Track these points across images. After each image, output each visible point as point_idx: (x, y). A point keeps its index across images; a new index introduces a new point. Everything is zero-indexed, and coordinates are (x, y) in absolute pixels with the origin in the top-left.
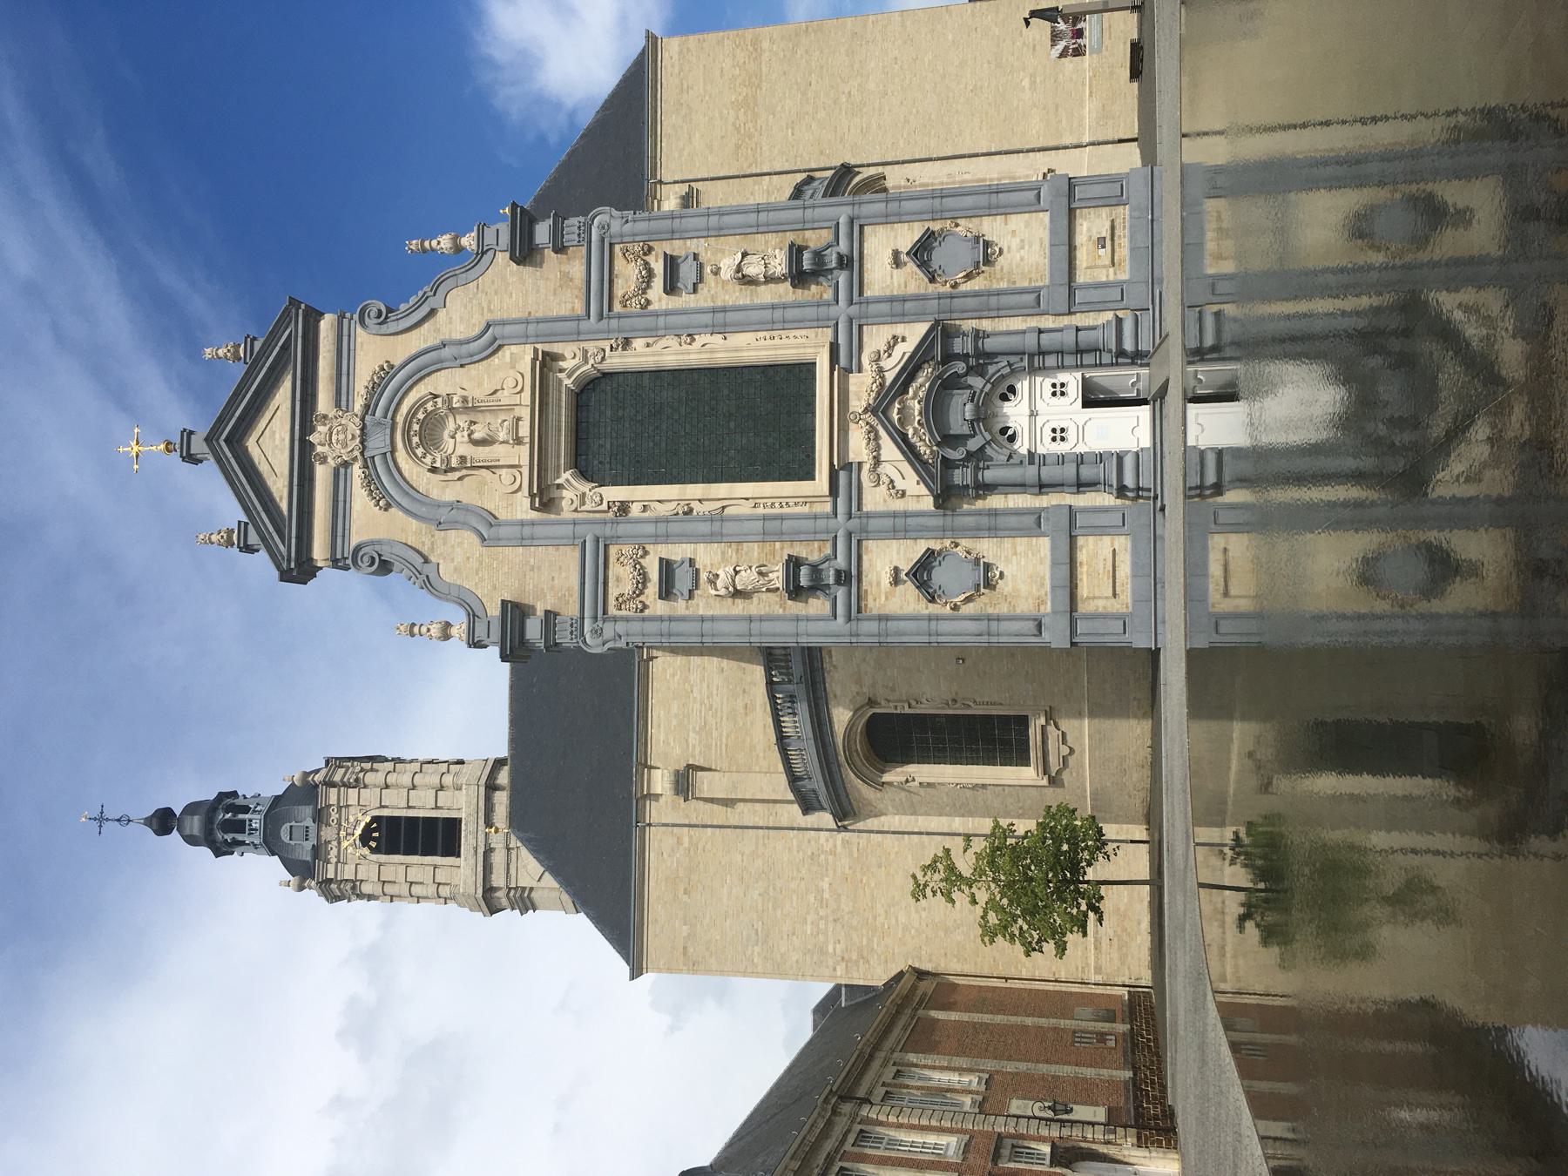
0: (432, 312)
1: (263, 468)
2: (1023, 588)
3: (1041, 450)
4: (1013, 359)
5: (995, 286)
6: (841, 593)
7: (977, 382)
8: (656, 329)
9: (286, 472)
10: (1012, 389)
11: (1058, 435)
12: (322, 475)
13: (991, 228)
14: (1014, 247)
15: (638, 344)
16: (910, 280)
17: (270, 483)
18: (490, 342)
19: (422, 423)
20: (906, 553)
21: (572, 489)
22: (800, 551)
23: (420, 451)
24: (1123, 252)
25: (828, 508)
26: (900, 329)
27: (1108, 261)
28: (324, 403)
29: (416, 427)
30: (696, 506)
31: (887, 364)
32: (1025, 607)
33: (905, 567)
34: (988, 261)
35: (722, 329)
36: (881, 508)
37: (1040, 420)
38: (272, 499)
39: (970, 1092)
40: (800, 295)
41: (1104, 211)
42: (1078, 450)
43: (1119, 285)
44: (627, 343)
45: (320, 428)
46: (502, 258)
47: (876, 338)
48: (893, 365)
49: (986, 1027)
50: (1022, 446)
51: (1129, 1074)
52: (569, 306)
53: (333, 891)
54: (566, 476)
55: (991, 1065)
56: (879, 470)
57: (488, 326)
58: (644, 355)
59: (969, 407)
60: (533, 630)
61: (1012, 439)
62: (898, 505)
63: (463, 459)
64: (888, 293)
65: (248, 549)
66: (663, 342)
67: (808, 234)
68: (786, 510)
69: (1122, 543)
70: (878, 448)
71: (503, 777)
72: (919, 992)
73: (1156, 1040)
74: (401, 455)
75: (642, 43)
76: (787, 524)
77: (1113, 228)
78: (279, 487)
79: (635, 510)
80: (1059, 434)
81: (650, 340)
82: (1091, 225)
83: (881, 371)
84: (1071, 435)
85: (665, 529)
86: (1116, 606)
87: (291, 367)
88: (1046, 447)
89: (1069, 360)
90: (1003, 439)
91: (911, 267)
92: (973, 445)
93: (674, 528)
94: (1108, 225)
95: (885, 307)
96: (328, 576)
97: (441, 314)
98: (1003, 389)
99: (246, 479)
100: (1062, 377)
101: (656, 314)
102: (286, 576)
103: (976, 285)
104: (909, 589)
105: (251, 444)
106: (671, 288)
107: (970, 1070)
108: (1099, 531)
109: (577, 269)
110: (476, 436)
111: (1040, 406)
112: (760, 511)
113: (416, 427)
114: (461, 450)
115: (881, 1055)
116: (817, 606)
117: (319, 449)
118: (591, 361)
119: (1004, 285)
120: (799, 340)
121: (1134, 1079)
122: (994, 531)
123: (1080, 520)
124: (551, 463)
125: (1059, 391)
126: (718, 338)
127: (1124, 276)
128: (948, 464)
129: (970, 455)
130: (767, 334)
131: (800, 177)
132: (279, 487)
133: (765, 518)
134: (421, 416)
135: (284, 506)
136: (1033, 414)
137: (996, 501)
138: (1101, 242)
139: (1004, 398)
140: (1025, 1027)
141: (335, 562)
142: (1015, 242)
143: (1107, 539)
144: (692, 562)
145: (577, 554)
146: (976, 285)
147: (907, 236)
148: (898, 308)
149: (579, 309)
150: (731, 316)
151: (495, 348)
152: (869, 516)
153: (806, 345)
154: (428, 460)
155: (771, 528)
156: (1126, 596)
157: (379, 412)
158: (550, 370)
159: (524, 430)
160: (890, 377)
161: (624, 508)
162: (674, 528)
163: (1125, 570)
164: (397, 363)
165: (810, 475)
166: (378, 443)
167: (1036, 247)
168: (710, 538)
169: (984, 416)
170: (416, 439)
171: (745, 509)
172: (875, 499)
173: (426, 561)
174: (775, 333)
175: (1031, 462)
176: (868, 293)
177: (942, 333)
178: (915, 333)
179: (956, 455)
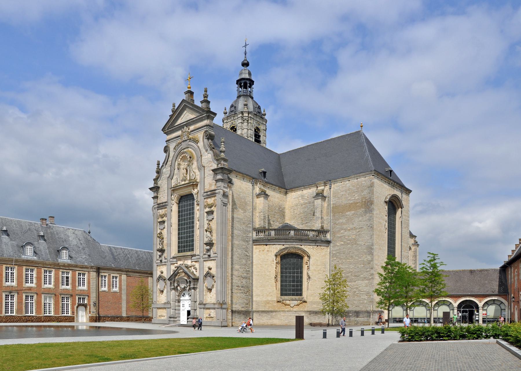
13: (214, 290)
15: (198, 207)
22: (166, 252)
31: (192, 268)
44: (198, 205)
47: (197, 265)
55: (124, 292)
57: (204, 167)
58: (196, 208)
83: (191, 267)
84: (183, 308)
124: (178, 191)
136: (186, 300)
138: (210, 315)
142: (211, 296)
144: (164, 228)
146: (205, 288)
155: (169, 245)
163: (163, 318)
165: (179, 252)
173: (166, 164)
177: (196, 280)
178: (197, 274)
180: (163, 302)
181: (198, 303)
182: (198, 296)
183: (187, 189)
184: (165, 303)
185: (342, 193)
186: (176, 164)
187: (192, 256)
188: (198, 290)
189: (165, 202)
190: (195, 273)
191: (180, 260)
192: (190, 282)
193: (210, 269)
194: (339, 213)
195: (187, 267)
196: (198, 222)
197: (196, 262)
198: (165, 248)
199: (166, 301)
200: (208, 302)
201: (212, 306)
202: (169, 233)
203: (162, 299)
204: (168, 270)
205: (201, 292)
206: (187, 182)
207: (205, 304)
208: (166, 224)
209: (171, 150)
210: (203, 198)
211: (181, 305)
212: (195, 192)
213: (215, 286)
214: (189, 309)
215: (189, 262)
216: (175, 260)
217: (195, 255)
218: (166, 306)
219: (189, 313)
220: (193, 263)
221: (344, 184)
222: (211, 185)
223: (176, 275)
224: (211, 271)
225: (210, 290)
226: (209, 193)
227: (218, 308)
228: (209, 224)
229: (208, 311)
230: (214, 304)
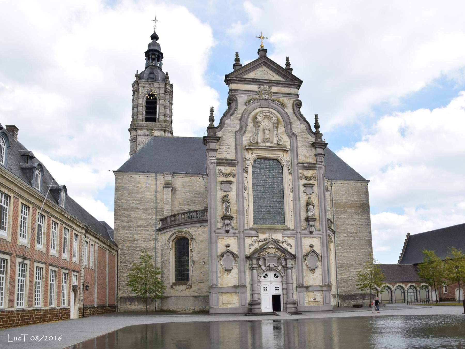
0: (299, 120)
1: (256, 71)
2: (225, 280)
3: (261, 284)
4: (285, 277)
5: (304, 272)
6: (223, 231)
7: (280, 268)
8: (294, 182)
9: (256, 78)
10: (277, 277)
11: (265, 289)
12: (254, 87)
13: (319, 271)
14: (314, 277)
15: (290, 177)
16: (306, 249)
17: (252, 73)
18: (291, 135)
19: (269, 116)
20: (234, 248)
21: (251, 157)
23: (261, 115)
24: (312, 304)
25: (246, 227)
26: (293, 247)
27: (309, 300)
28: (275, 89)
29: (268, 114)
30: (246, 192)
32: (220, 281)
33: (230, 248)
34: (311, 270)
35: (294, 199)
36: (246, 242)
37: (269, 284)
38: (248, 73)
39: (89, 265)
40: (303, 221)
41: (322, 299)
42: (261, 294)
43: (304, 303)
45: (268, 87)
46: (313, 140)
47: (292, 241)
48: (284, 245)
49: (105, 269)
50: (262, 279)
51: (96, 306)
52: (300, 158)
53: (136, 85)
54: (255, 156)
55: (96, 270)
56: (257, 242)
59: (273, 266)
60: (212, 145)
61: (264, 277)
62: (247, 246)
63: (259, 127)
64: (303, 244)
65: (234, 66)
66: (291, 184)
67: (319, 223)
68: (245, 216)
69: (237, 305)
70: (262, 241)
71: (168, 135)
72: (113, 251)
73: (104, 313)
74: (259, 109)
75: (367, 179)
76: (242, 216)
77: (318, 301)
78: (251, 75)
79: (245, 175)
80: (265, 289)
81: (291, 180)
82: (319, 296)
84: (265, 292)
85: (241, 182)
86: (220, 303)
87: (284, 80)
88: (262, 286)
89: (285, 291)
90: (264, 274)
91: (309, 249)
92: (263, 267)
93: (240, 185)
94: (319, 300)
95: (299, 243)
96: (227, 88)
97: (299, 122)
98: (278, 274)
99: (253, 66)
100: (280, 289)
101: (298, 182)
102: (227, 76)
103: (305, 268)
104: (225, 249)
105: (264, 68)
106: (305, 185)
107: (95, 265)
108: (240, 300)
109: (311, 160)
110: (266, 131)
111: (273, 284)
112: (245, 210)
113: (268, 114)
114: (261, 126)
115: (96, 240)
116: (220, 225)
117: (262, 87)
118: (286, 163)
119: (304, 274)
120: (291, 221)
121: (94, 307)
122: (240, 271)
123: (243, 295)
124: (258, 152)
125: (277, 289)
126: (291, 199)
127: (306, 304)
128: (258, 260)
129: (260, 266)
130: (293, 212)
131: (332, 221)
132: (251, 75)
133: (243, 211)
134: (271, 116)
135: (246, 77)
136: (271, 282)
137: (248, 273)
138: (315, 299)
139: (275, 275)
140: (106, 279)
141: (230, 90)
143: (238, 301)
145: (233, 158)
146: (305, 268)
147: (317, 249)
148: (299, 246)
149: (300, 161)
150: (298, 202)
151: (289, 137)
152: (244, 239)
153: (290, 222)
154: (259, 118)
155: (241, 212)
156: (223, 306)
157: (272, 104)
158: (283, 152)
159: (268, 144)
160: (281, 245)
161: (246, 172)
162: (240, 185)
163: (230, 306)
164: (285, 109)
166: (263, 102)
167: (314, 283)
168: (238, 195)
169: (270, 269)
170: (264, 114)
171: (246, 205)
172: (248, 241)
173: (231, 115)
174: (293, 214)
175: (258, 282)
176: (303, 239)
178: (292, 251)
179: (261, 262)
180: (230, 285)
181: (295, 286)
182: (294, 277)
183: (273, 152)
184: (236, 287)
185: (342, 193)
186: (250, 120)
187: (284, 230)
188: (294, 270)
189: (232, 160)
190: (289, 250)
191: (264, 233)
192: (286, 260)
193: (311, 246)
194: (341, 209)
195: (279, 241)
196: (291, 194)
197: (289, 237)
198: (234, 215)
199: (237, 284)
200: (309, 285)
201: (319, 288)
202: (241, 197)
203: (231, 280)
204: (241, 245)
205: (300, 274)
206: (272, 145)
207: (307, 287)
208: (234, 186)
209: (239, 102)
210: (296, 168)
211: (262, 289)
212: (285, 158)
213: (320, 266)
214: (277, 293)
215: (278, 236)
216: (253, 232)
217: (289, 229)
218: (238, 288)
219: (276, 299)
220: (285, 238)
221: (343, 186)
222: (307, 157)
223: (262, 252)
224: (314, 249)
225: (313, 270)
226: (305, 165)
227: (326, 291)
228: (310, 198)
229: (311, 295)
230: (321, 286)
